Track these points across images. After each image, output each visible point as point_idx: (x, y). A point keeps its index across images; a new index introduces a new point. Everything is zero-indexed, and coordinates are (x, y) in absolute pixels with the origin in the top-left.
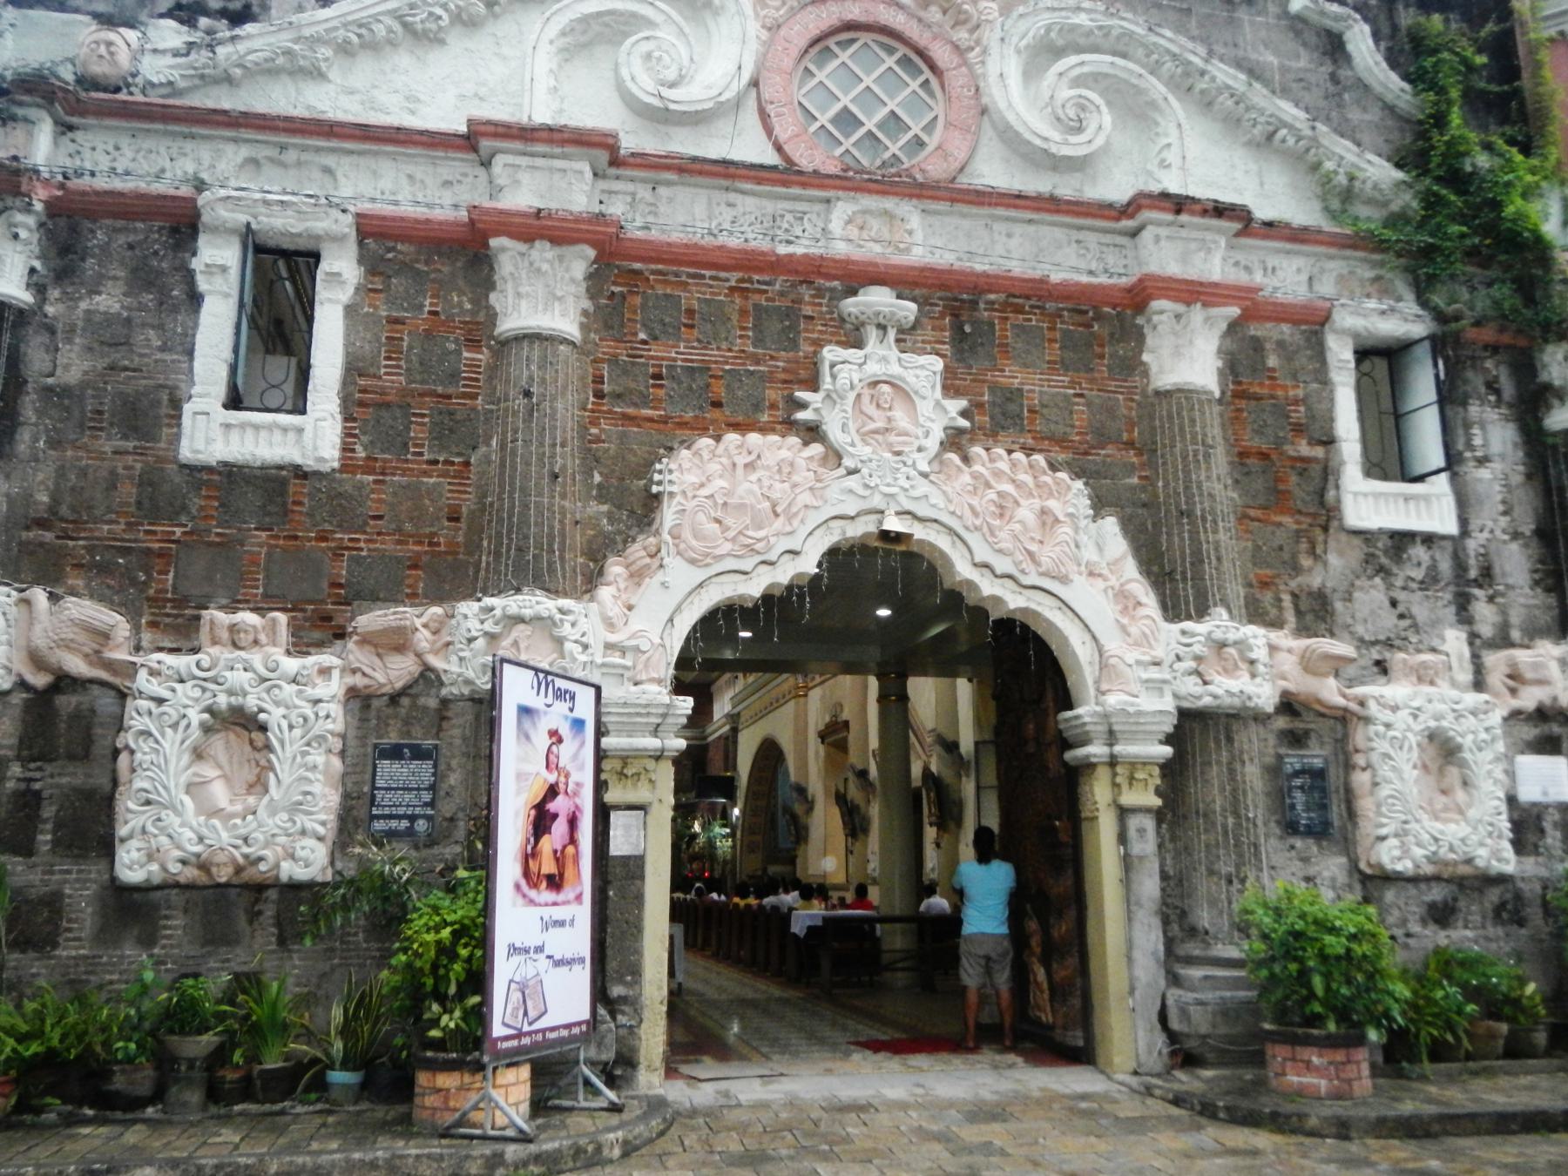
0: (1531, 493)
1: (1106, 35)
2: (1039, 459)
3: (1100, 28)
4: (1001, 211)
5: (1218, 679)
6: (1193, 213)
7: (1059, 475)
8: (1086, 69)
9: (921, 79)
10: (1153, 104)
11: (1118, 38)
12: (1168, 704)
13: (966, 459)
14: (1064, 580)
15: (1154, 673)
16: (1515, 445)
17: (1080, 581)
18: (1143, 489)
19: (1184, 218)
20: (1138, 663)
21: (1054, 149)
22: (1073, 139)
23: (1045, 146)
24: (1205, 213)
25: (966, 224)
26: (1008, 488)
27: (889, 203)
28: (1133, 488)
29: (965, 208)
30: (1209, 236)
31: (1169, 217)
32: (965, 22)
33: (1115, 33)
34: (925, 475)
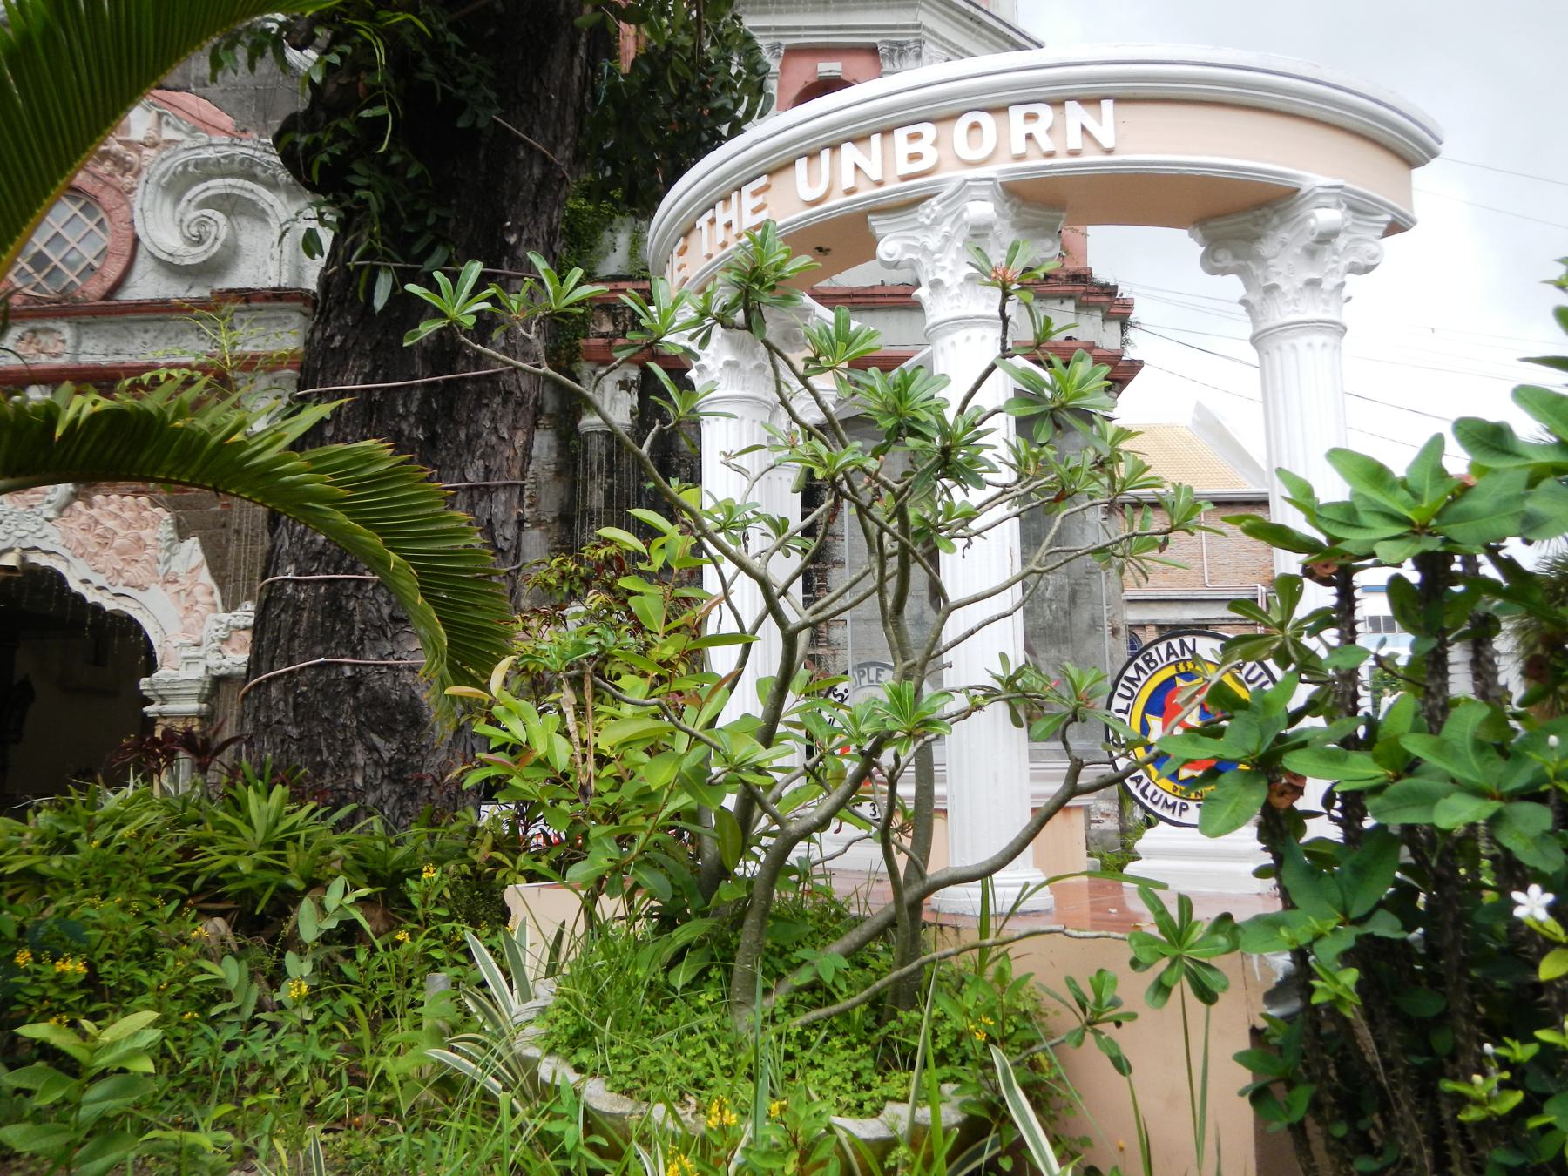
0: (560, 487)
1: (233, 161)
2: (143, 500)
3: (225, 157)
4: (130, 317)
5: (229, 654)
6: (259, 300)
7: (158, 510)
8: (209, 193)
9: (97, 219)
10: (263, 211)
11: (242, 162)
12: (198, 672)
13: (90, 505)
14: (142, 588)
15: (193, 652)
16: (550, 448)
17: (155, 588)
18: (222, 514)
19: (254, 305)
20: (182, 645)
21: (177, 262)
22: (194, 250)
23: (170, 259)
24: (267, 298)
25: (114, 327)
26: (110, 523)
27: (50, 324)
28: (216, 513)
29: (106, 318)
30: (283, 314)
31: (244, 306)
32: (130, 169)
33: (237, 159)
34: (49, 520)
